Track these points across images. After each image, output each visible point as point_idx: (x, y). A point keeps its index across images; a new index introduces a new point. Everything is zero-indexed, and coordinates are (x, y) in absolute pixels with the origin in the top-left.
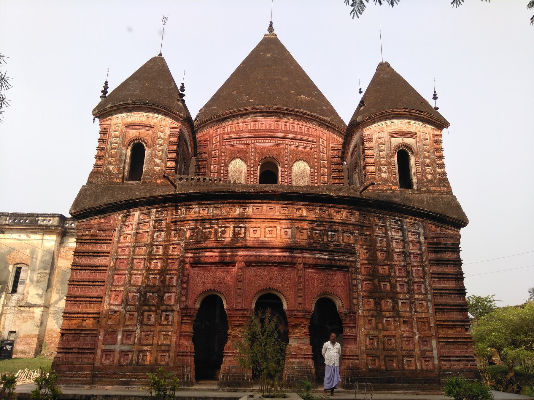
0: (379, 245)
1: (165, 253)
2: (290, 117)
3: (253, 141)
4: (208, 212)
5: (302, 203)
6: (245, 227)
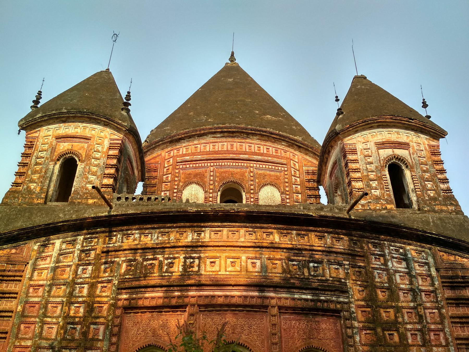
0: (377, 280)
1: (91, 294)
2: (255, 138)
3: (212, 164)
4: (152, 238)
5: (273, 226)
6: (199, 258)
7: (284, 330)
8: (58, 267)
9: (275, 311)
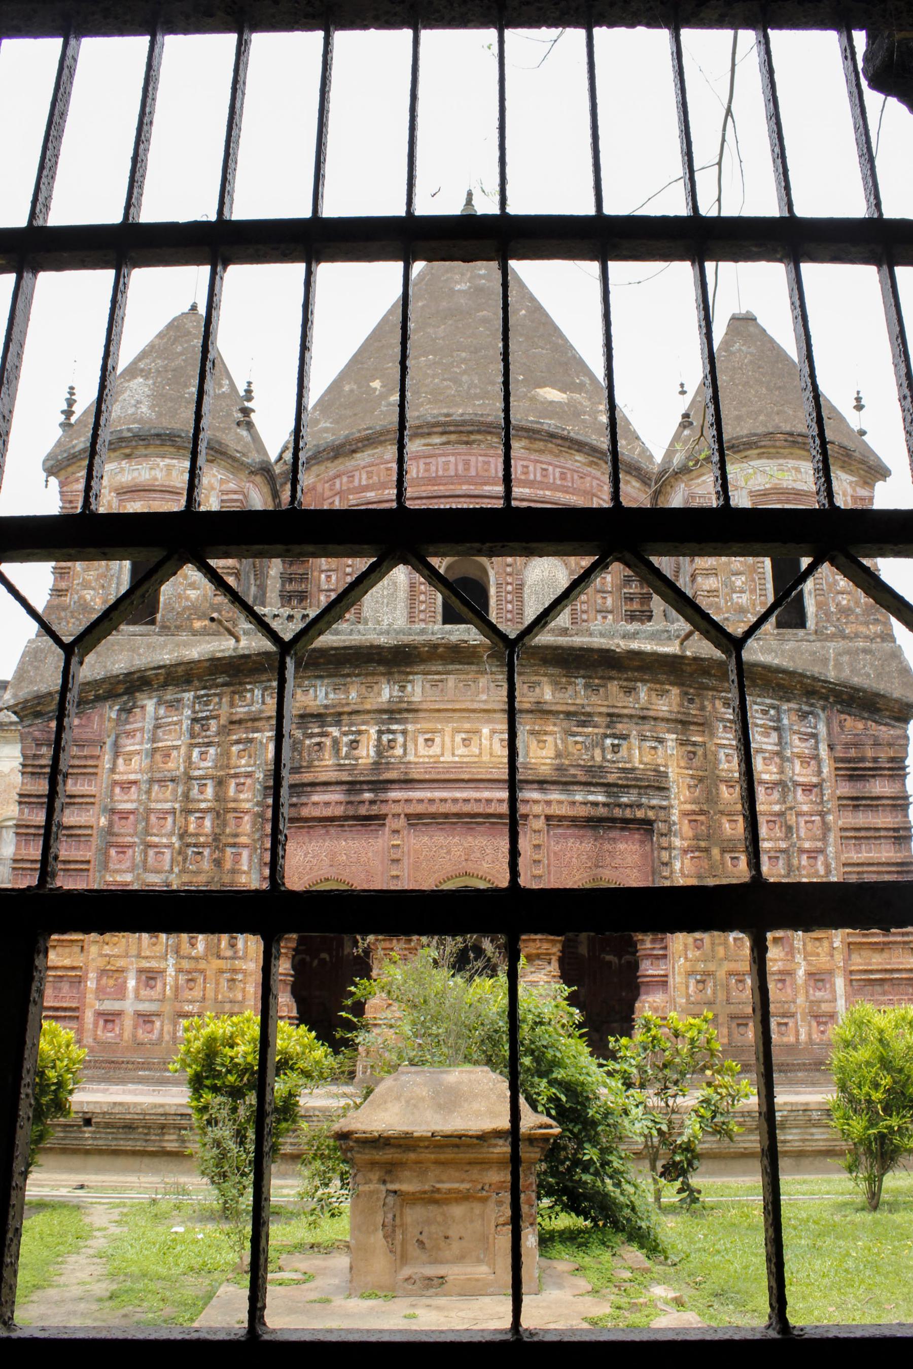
1: (220, 797)
6: (404, 732)
7: (555, 853)
8: (155, 750)
9: (540, 824)
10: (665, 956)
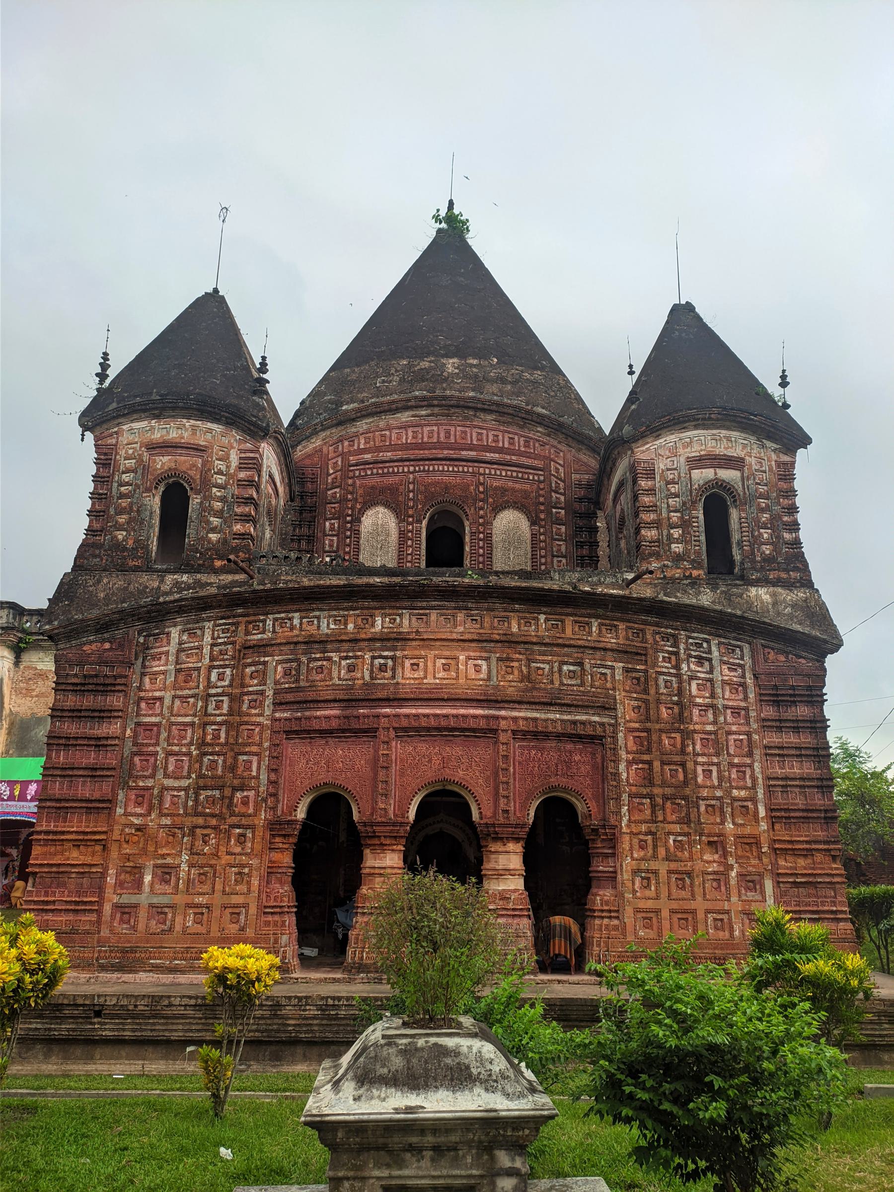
7: (520, 763)
10: (613, 855)
